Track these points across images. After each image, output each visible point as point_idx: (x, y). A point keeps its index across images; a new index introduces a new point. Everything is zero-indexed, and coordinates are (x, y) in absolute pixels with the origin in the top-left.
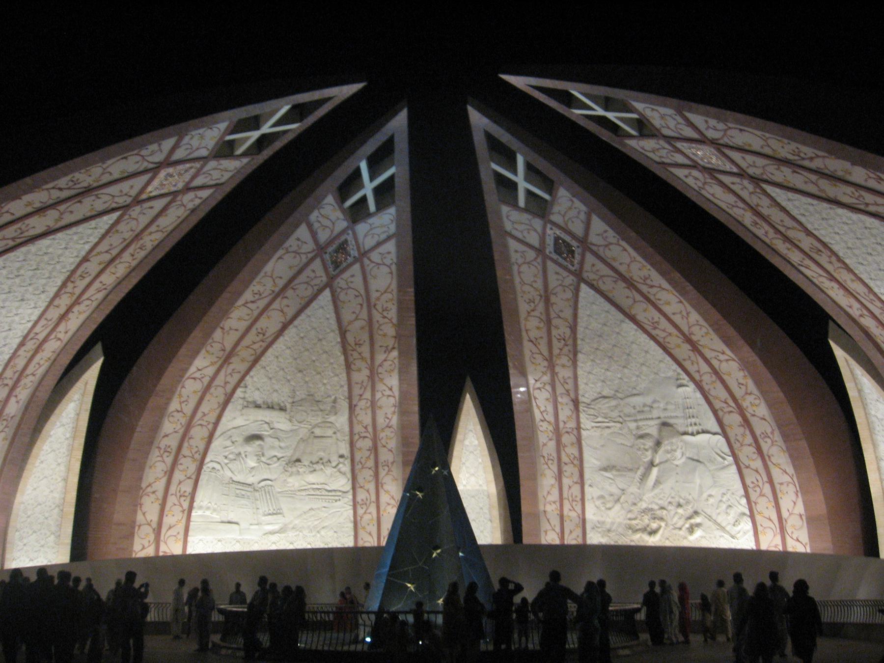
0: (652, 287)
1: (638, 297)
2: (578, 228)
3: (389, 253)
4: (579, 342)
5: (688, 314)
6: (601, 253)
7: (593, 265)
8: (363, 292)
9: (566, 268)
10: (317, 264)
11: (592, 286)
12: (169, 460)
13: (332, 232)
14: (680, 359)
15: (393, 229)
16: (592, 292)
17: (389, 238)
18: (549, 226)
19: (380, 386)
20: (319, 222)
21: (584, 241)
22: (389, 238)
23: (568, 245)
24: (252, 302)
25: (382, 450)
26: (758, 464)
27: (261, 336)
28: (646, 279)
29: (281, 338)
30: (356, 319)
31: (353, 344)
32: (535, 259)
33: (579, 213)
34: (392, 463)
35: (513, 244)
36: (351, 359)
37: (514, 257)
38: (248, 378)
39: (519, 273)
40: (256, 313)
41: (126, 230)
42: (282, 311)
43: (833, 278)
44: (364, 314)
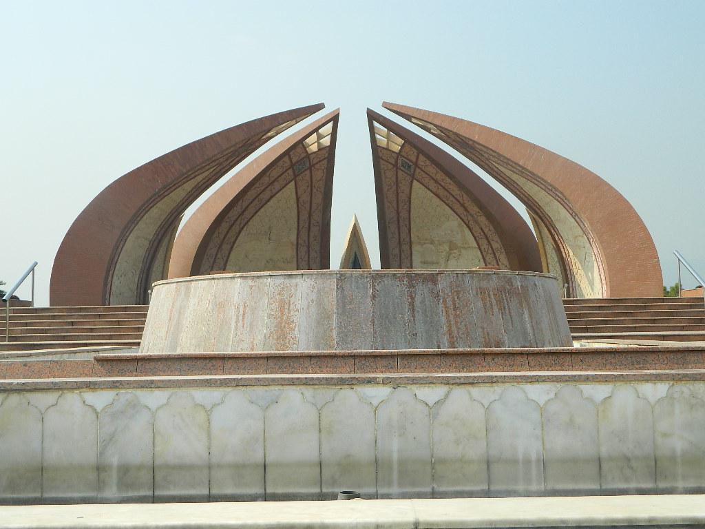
2: (413, 159)
9: (406, 173)
10: (290, 171)
11: (417, 180)
12: (212, 261)
15: (327, 155)
16: (418, 183)
17: (325, 159)
19: (312, 221)
21: (416, 164)
22: (325, 159)
28: (443, 180)
36: (300, 210)
37: (382, 166)
39: (385, 173)
41: (218, 170)
43: (520, 191)
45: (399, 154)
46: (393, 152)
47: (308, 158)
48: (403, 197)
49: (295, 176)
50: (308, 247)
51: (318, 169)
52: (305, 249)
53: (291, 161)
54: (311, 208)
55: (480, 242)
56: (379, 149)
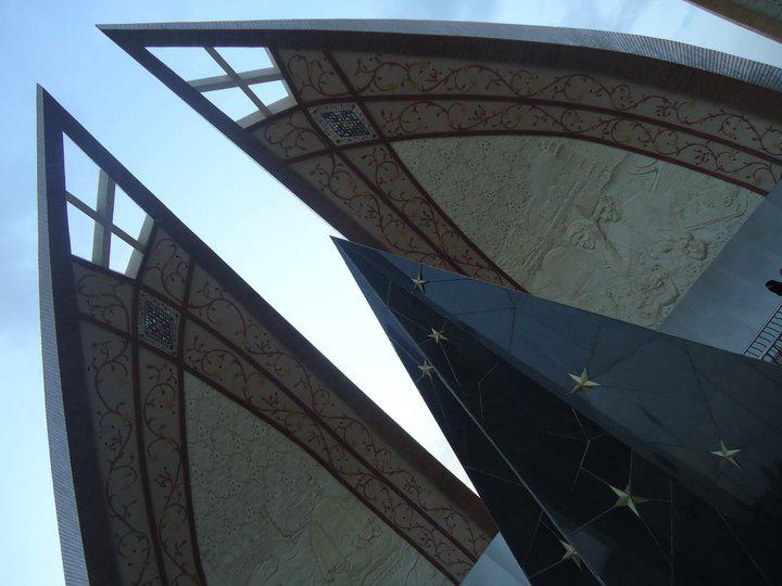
0: (446, 79)
1: (446, 104)
2: (335, 86)
3: (207, 284)
4: (443, 207)
5: (499, 76)
6: (378, 92)
7: (383, 113)
8: (222, 346)
10: (146, 357)
11: (401, 138)
13: (124, 307)
14: (533, 129)
16: (407, 144)
18: (311, 110)
19: (333, 424)
20: (99, 307)
21: (355, 96)
23: (345, 113)
24: (120, 456)
25: (392, 479)
26: (685, 138)
27: (168, 484)
29: (193, 469)
30: (246, 380)
31: (269, 407)
32: (334, 165)
33: (320, 67)
34: (413, 480)
35: (303, 169)
36: (281, 423)
37: (315, 180)
38: (200, 540)
39: (337, 196)
40: (136, 464)
42: (163, 438)
44: (249, 369)
45: (302, 102)
46: (289, 113)
47: (153, 293)
48: (414, 209)
49: (179, 362)
50: (378, 475)
51: (210, 304)
52: (375, 485)
53: (118, 333)
54: (297, 401)
55: (619, 137)
56: (259, 135)
